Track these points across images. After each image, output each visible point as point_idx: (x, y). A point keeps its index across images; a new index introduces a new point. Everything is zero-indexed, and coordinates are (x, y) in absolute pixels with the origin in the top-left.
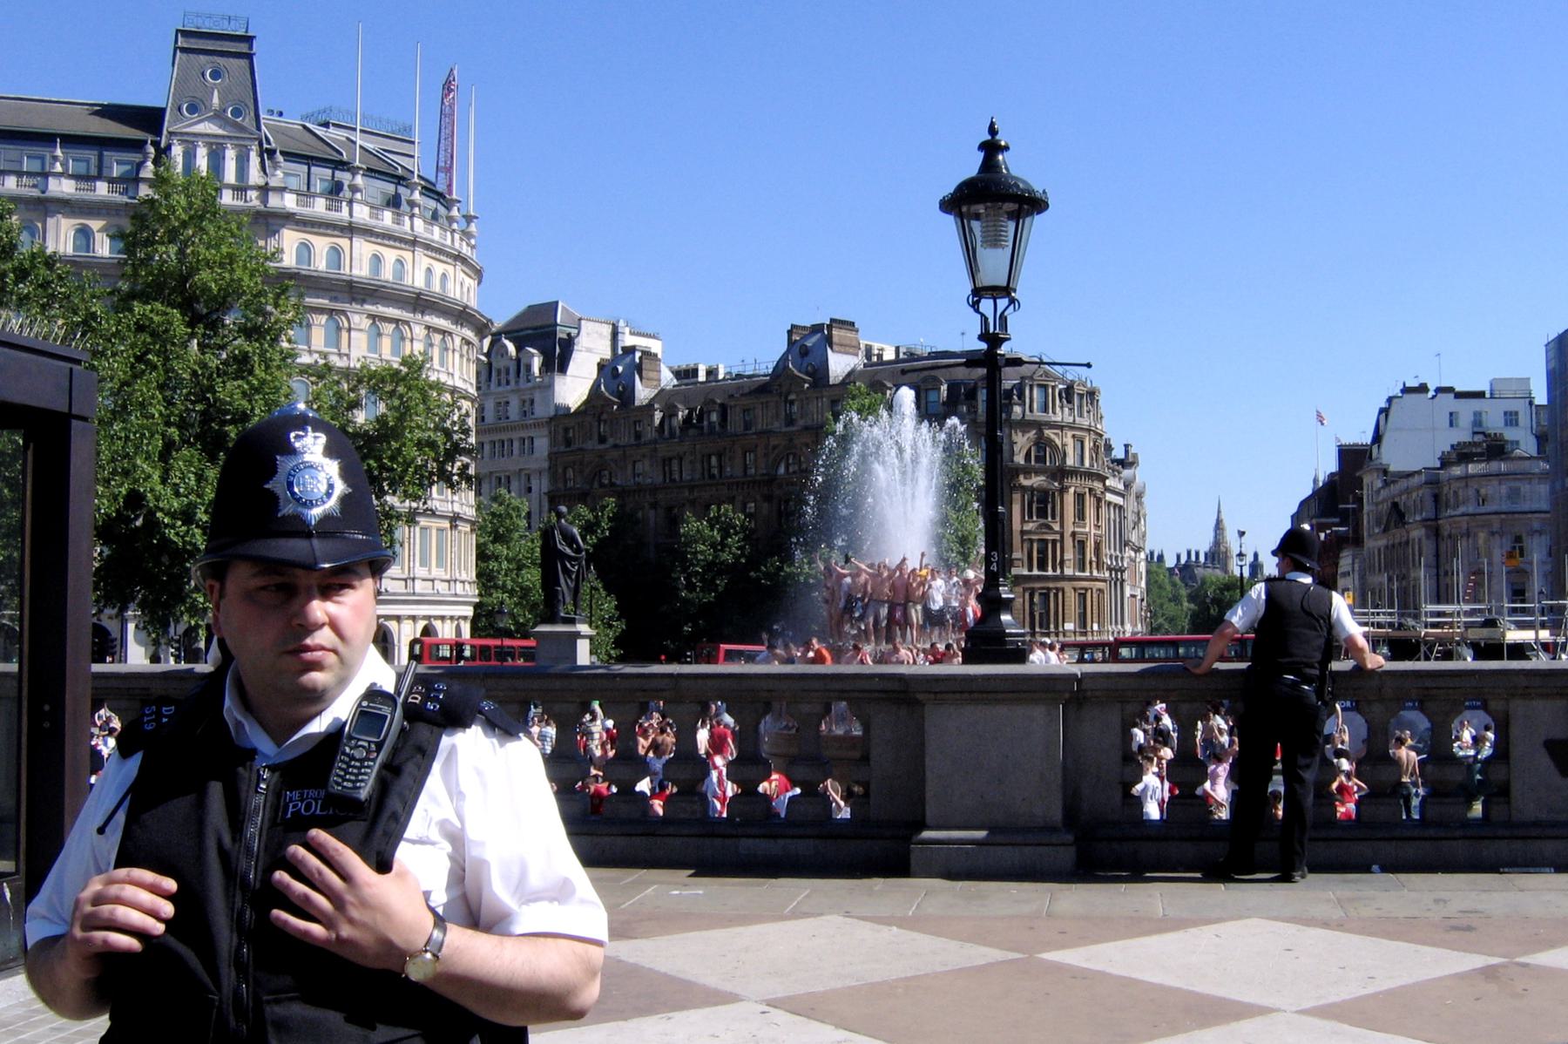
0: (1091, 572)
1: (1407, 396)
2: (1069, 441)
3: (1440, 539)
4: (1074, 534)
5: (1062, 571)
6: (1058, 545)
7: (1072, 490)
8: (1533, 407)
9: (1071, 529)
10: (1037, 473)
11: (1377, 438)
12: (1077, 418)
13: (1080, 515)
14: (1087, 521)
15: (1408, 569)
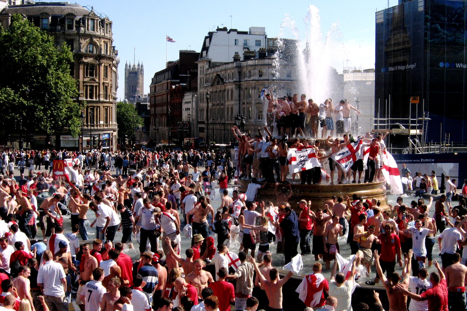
0: (109, 100)
1: (220, 32)
2: (102, 43)
3: (241, 90)
4: (104, 83)
5: (99, 99)
6: (98, 88)
7: (103, 65)
8: (267, 39)
9: (103, 81)
10: (90, 57)
11: (205, 48)
12: (106, 34)
13: (106, 75)
14: (108, 78)
15: (225, 101)
